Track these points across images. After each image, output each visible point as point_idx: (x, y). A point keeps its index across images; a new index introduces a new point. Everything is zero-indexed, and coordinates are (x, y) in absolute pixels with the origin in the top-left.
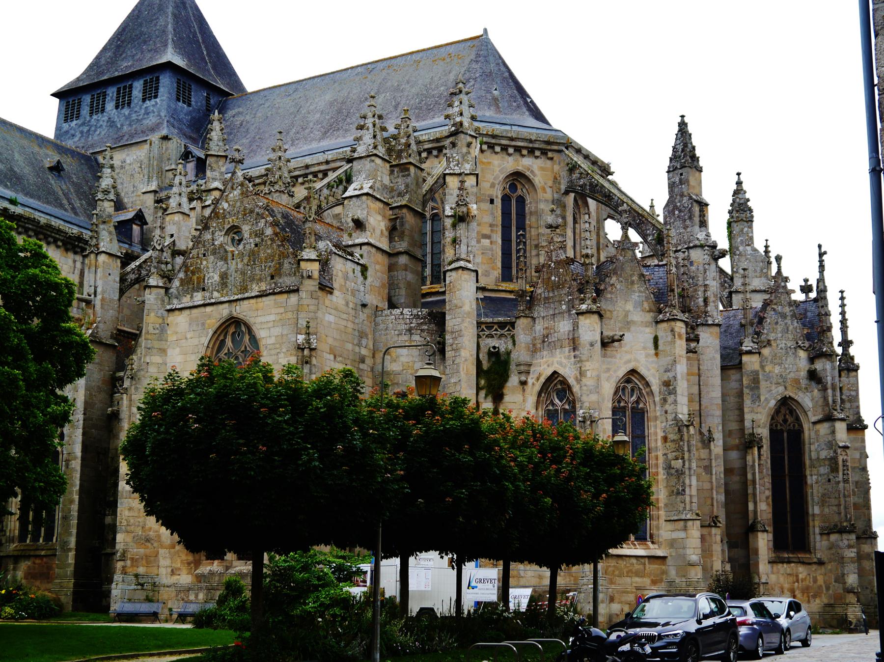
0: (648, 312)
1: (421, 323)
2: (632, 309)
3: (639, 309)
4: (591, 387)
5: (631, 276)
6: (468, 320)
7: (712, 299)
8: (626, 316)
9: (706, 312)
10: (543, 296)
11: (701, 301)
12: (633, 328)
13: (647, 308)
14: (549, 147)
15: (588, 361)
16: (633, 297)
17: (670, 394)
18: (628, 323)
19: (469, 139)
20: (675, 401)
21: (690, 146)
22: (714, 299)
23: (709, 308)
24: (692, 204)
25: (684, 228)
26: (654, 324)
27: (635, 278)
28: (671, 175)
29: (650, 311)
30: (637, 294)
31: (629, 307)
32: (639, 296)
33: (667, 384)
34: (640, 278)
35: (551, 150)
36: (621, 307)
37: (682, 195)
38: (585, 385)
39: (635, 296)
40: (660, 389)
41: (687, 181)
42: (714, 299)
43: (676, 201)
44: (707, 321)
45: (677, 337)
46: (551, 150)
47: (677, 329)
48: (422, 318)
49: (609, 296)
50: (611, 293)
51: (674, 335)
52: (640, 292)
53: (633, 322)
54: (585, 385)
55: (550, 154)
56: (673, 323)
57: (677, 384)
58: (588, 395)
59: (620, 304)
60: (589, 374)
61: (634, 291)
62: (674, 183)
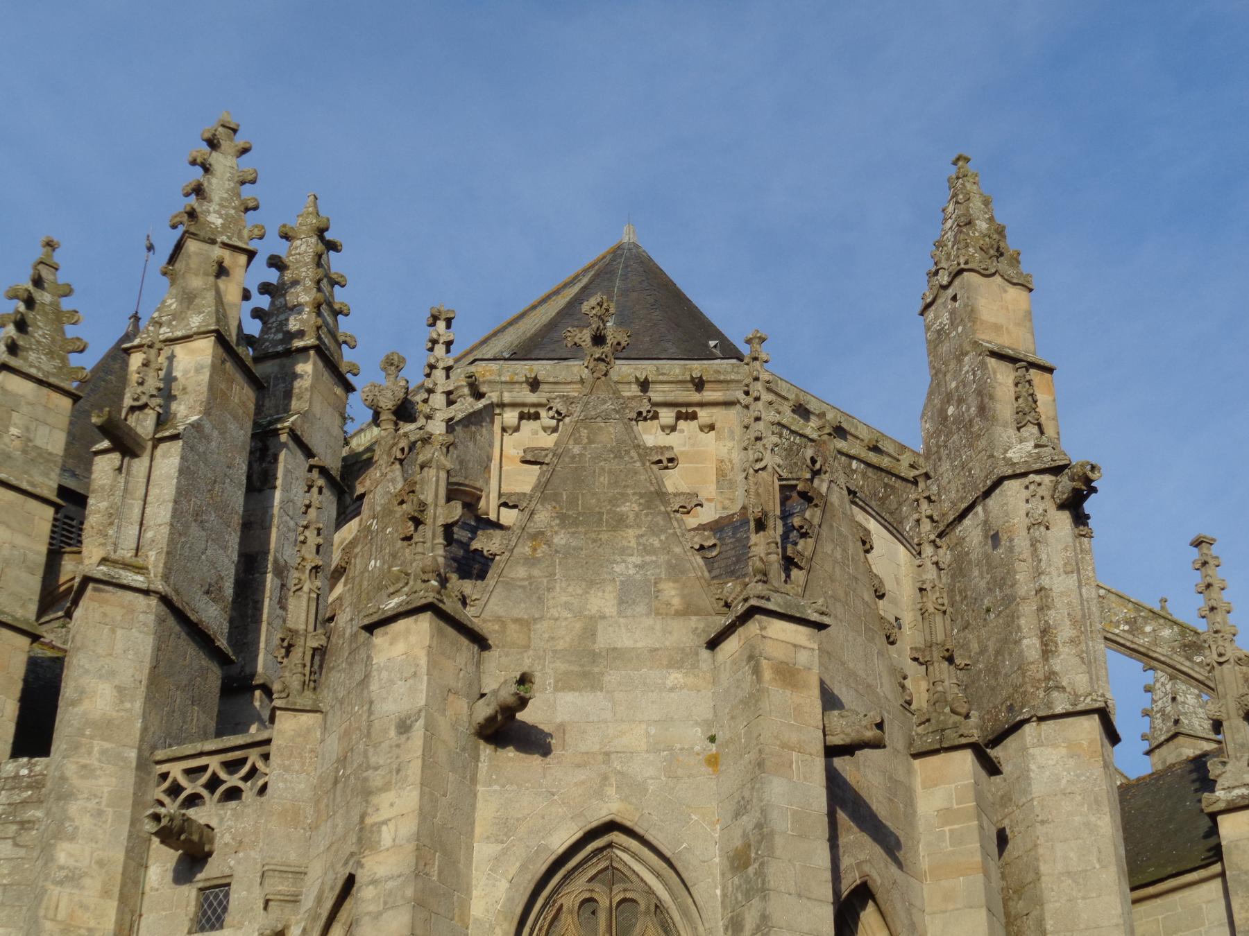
0: (678, 614)
1: (24, 802)
2: (609, 607)
3: (641, 608)
4: (390, 884)
5: (613, 501)
6: (98, 745)
7: (1065, 632)
8: (590, 632)
9: (1051, 675)
10: (348, 631)
11: (1030, 645)
12: (612, 678)
13: (676, 602)
14: (696, 397)
15: (386, 788)
16: (618, 568)
17: (748, 896)
18: (594, 657)
19: (217, 252)
20: (764, 917)
21: (982, 225)
22: (1073, 633)
23: (1057, 664)
24: (983, 365)
25: (971, 445)
26: (705, 654)
27: (629, 508)
28: (931, 314)
29: (688, 610)
30: (637, 559)
31: (603, 602)
32: (640, 567)
33: (739, 861)
34: (648, 505)
35: (702, 405)
36: (566, 606)
37: (960, 356)
38: (374, 882)
39: (627, 567)
40: (724, 888)
41: (972, 314)
42: (1073, 633)
43: (948, 377)
44: (1049, 705)
45: (767, 674)
46: (702, 405)
47: (771, 649)
48: (29, 787)
49: (521, 572)
50: (531, 561)
51: (757, 671)
52: (647, 550)
53: (617, 655)
54: (374, 882)
55: (704, 415)
56: (752, 627)
57: (771, 854)
58: (377, 916)
59: (564, 595)
60: (386, 835)
61: (623, 551)
62: (939, 332)
